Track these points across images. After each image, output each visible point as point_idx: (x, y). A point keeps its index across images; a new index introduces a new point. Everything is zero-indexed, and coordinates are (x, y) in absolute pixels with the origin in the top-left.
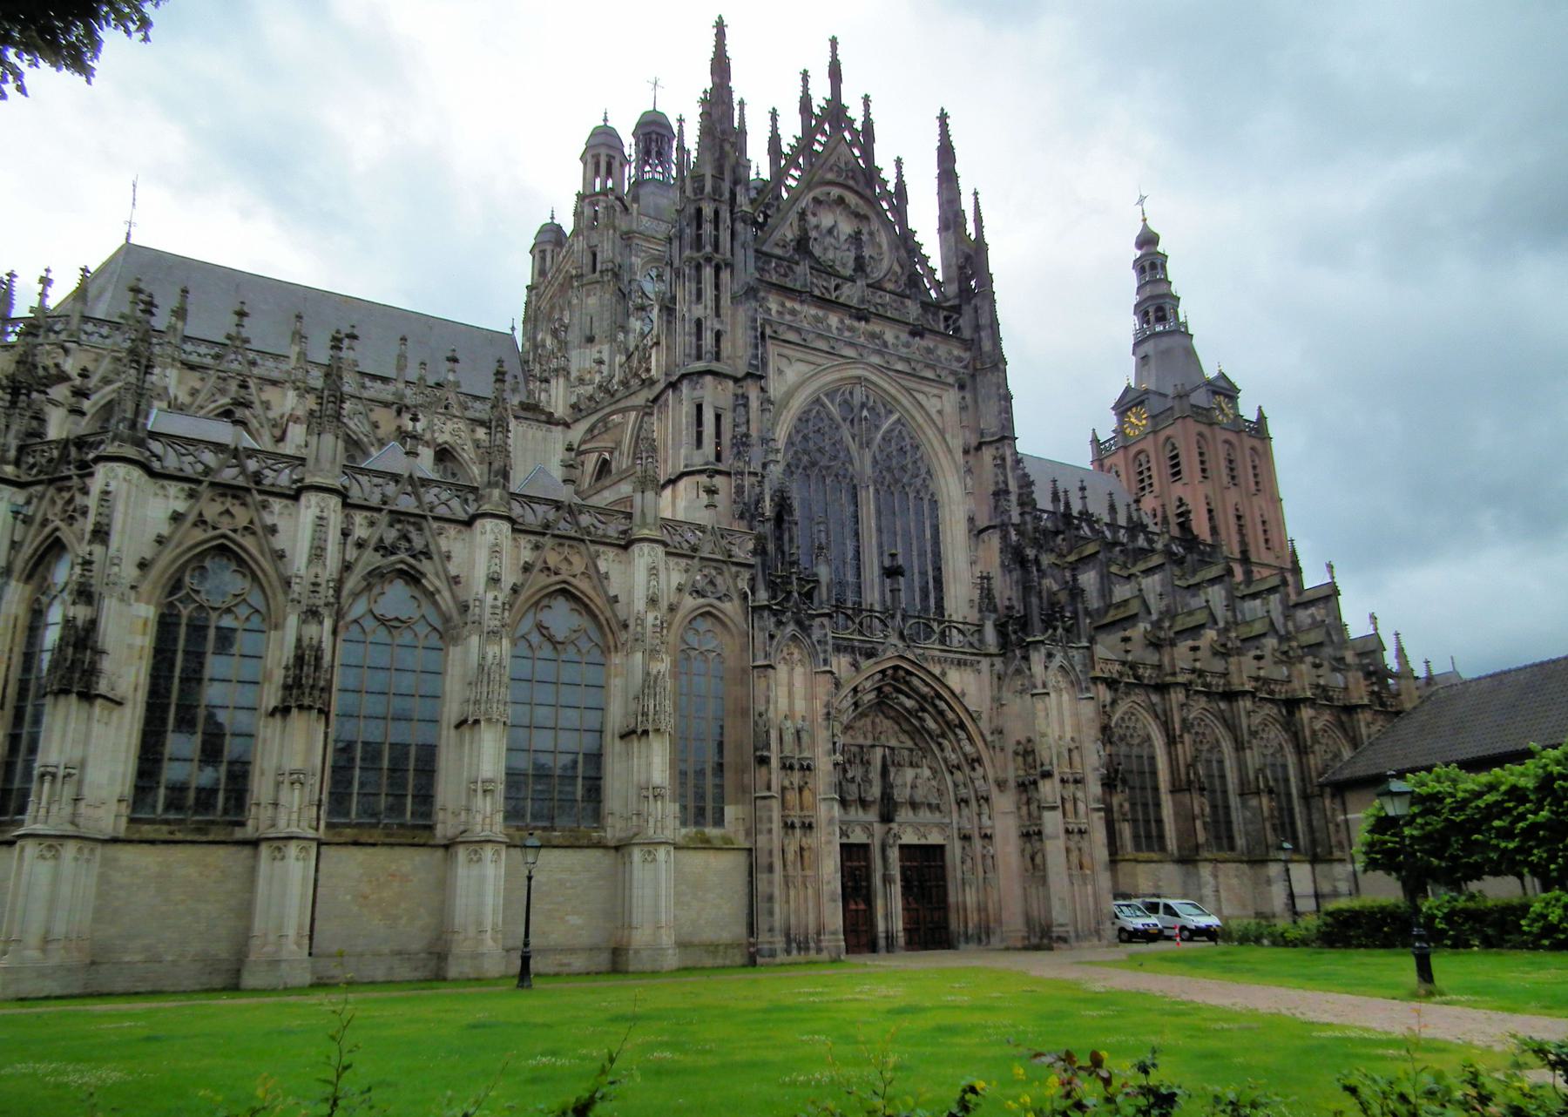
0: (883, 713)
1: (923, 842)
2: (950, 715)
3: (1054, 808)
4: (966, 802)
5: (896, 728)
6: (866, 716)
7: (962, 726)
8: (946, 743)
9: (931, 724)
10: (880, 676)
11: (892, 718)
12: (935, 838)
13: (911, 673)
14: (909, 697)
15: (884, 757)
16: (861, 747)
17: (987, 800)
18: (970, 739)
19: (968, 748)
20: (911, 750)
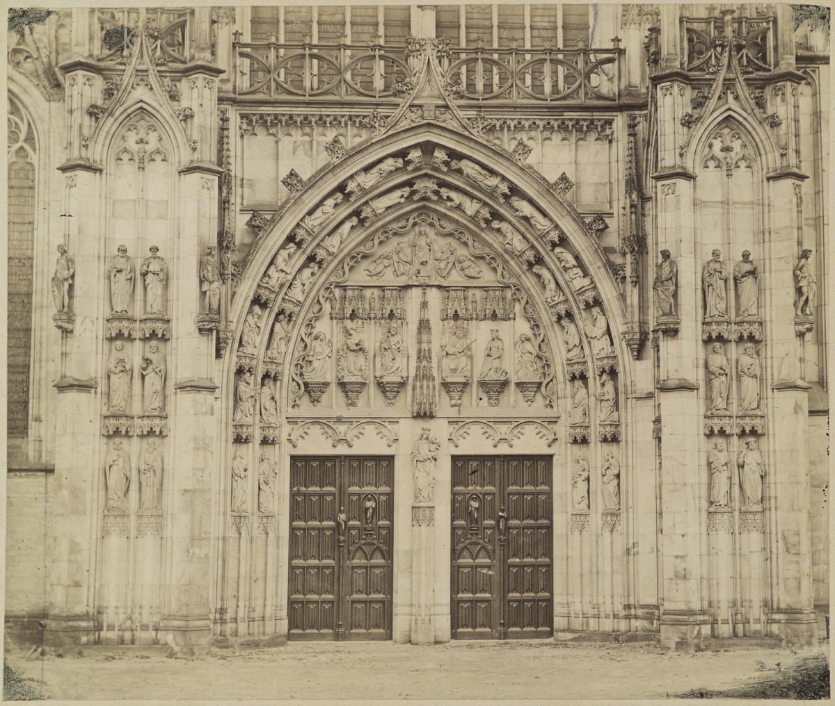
0: (431, 225)
1: (503, 450)
2: (541, 223)
3: (684, 387)
4: (583, 378)
5: (462, 252)
6: (395, 234)
7: (563, 241)
8: (546, 274)
9: (518, 244)
10: (389, 165)
11: (451, 235)
12: (529, 443)
13: (461, 157)
14: (472, 197)
15: (424, 305)
16: (382, 288)
17: (613, 373)
18: (580, 264)
19: (580, 282)
20: (485, 289)
